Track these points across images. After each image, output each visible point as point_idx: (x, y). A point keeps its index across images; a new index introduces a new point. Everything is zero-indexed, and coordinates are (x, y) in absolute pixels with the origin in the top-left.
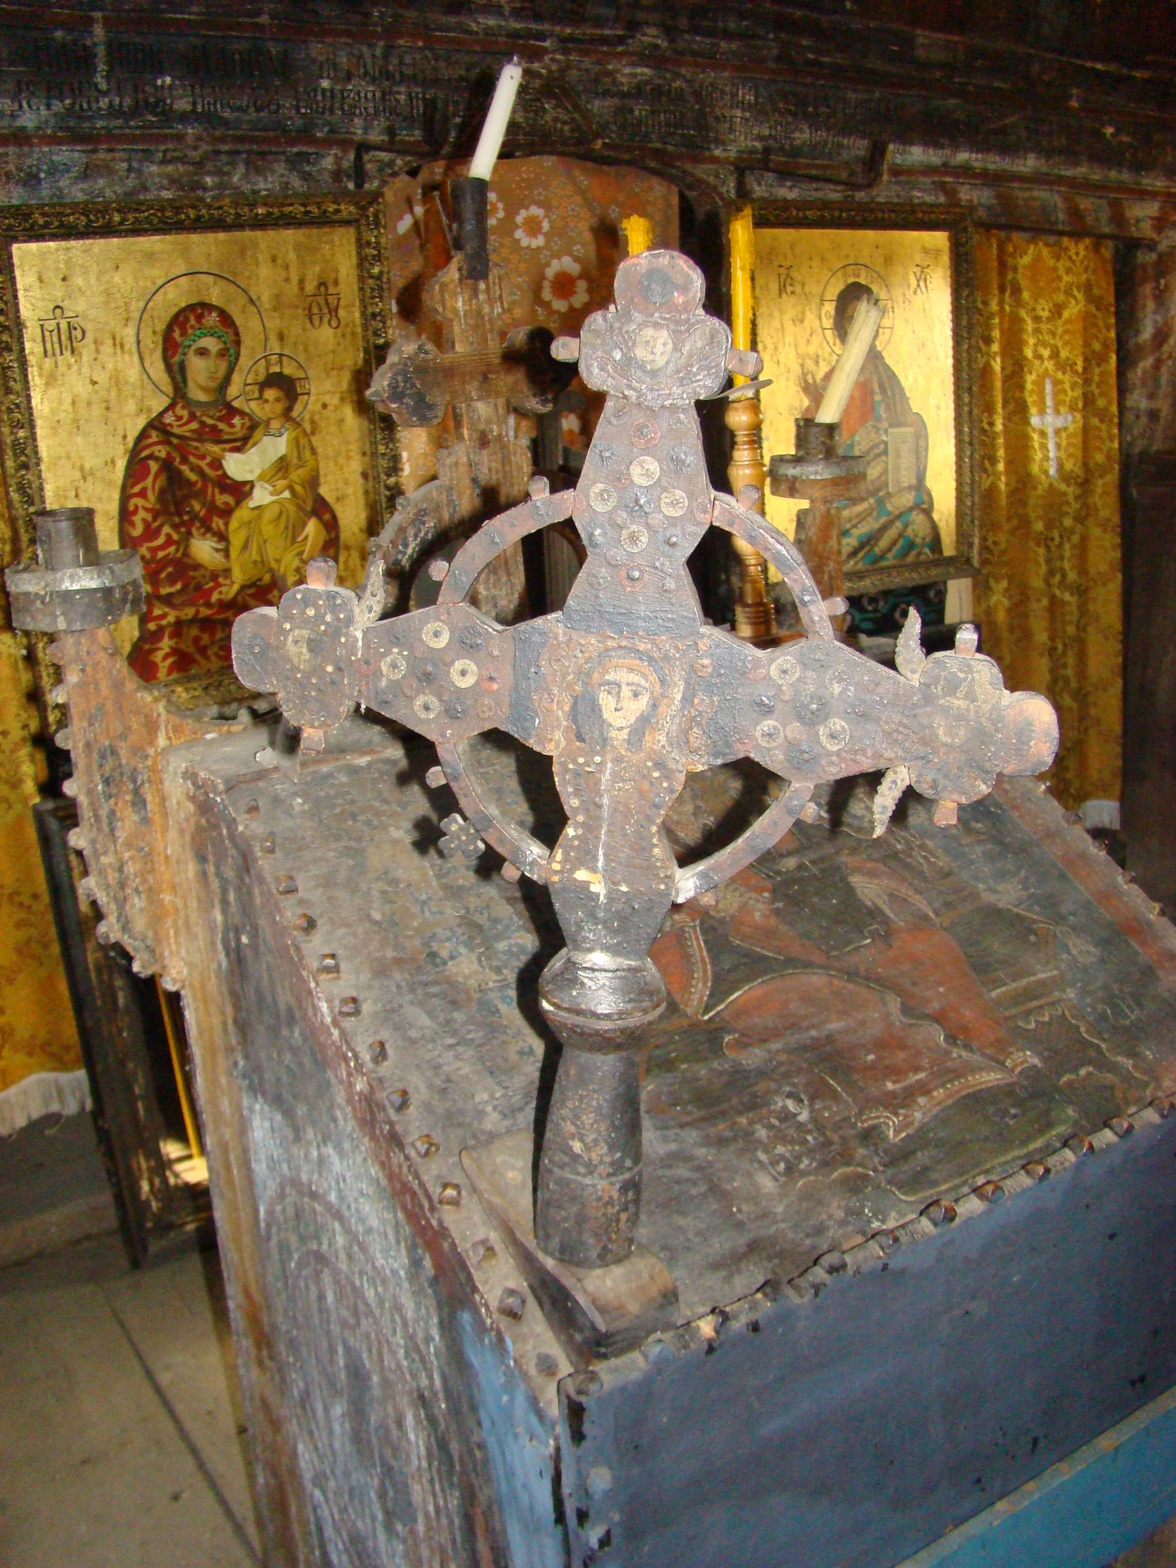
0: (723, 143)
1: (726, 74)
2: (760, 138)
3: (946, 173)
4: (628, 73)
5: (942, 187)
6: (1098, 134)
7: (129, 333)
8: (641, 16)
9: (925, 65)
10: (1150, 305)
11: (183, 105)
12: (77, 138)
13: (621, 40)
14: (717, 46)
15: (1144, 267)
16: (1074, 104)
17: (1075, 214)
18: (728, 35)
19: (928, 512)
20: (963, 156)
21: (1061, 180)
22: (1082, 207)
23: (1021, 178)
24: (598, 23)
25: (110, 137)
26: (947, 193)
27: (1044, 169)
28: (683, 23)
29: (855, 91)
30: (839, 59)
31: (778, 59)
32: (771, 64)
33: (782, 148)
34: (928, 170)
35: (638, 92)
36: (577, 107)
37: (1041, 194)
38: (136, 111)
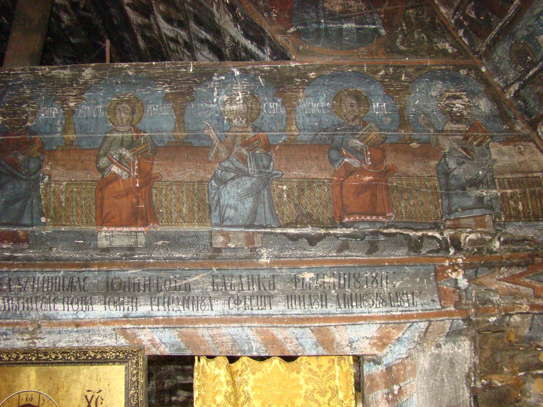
3: (129, 322)
5: (123, 331)
6: (295, 280)
9: (107, 250)
15: (372, 378)
20: (144, 309)
21: (253, 318)
22: (280, 337)
23: (208, 320)
26: (126, 336)
27: (235, 311)
29: (42, 272)
30: (31, 253)
34: (106, 322)
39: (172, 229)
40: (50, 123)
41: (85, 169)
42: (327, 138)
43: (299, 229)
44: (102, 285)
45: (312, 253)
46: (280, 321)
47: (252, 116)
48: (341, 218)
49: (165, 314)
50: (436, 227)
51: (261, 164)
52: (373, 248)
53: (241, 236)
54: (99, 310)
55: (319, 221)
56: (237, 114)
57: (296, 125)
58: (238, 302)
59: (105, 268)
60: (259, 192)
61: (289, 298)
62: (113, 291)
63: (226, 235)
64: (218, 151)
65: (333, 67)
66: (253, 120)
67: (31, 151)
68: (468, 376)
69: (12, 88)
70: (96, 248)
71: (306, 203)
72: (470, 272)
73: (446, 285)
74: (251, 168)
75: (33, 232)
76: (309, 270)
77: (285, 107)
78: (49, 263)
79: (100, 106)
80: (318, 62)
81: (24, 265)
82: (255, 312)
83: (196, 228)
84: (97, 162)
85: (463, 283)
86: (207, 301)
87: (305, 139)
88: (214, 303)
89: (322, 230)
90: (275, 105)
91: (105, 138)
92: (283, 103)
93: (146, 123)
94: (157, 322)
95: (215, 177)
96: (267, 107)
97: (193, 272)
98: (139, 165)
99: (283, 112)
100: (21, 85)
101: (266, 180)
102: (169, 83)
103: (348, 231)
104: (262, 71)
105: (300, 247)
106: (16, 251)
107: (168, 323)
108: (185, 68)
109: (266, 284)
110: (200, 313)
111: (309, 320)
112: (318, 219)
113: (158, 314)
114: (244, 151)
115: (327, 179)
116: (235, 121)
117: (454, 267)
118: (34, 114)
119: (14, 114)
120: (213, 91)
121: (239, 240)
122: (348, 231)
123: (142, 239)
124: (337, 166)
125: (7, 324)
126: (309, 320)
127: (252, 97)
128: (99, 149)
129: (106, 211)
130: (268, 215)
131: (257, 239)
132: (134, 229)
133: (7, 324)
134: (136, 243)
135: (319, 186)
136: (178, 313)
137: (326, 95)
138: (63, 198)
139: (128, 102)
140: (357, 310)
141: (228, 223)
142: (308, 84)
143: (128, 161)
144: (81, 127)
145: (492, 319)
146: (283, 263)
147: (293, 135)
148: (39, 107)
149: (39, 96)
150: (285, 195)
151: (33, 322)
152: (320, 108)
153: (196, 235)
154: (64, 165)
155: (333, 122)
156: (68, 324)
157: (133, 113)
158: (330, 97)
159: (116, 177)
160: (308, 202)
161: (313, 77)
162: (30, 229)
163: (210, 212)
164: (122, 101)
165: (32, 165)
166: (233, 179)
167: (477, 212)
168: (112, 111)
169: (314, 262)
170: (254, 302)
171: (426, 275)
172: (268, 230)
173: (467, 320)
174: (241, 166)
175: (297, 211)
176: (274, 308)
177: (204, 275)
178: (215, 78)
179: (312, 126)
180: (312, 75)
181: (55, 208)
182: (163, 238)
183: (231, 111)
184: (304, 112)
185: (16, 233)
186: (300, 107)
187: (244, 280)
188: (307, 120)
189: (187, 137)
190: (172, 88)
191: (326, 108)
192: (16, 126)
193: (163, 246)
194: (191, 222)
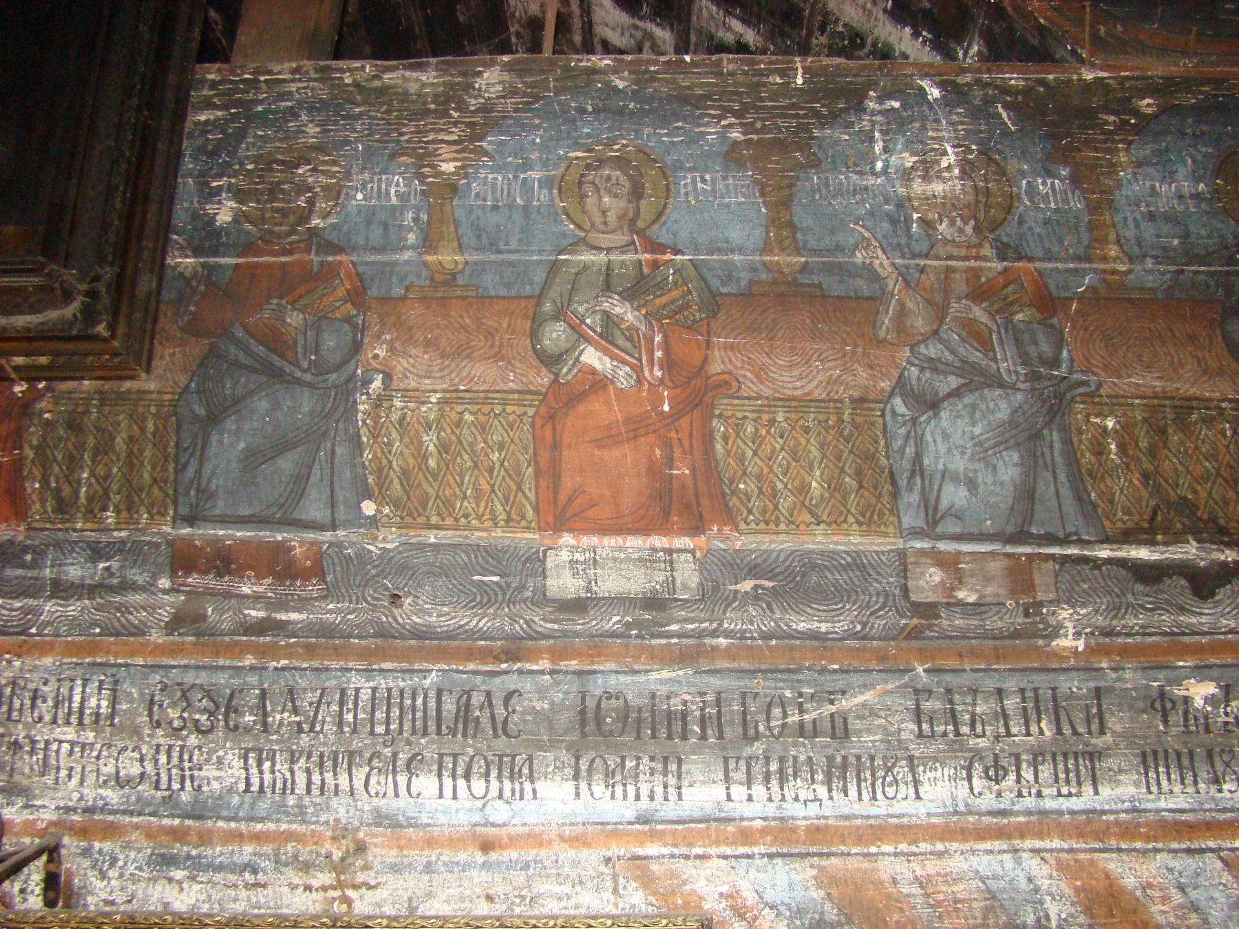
0: (25, 792)
1: (48, 661)
2: (120, 781)
3: (653, 836)
6: (1162, 704)
9: (578, 606)
14: (37, 612)
18: (61, 590)
21: (1043, 823)
22: (1130, 882)
23: (906, 831)
27: (987, 801)
29: (368, 673)
30: (330, 612)
31: (177, 622)
32: (156, 637)
33: (170, 800)
39: (781, 543)
40: (385, 222)
41: (498, 356)
42: (1212, 283)
43: (1163, 548)
44: (566, 718)
45: (1203, 620)
46: (1128, 831)
47: (990, 213)
49: (771, 810)
51: (1032, 350)
53: (995, 566)
54: (555, 799)
55: (1217, 524)
56: (948, 206)
57: (1118, 242)
58: (996, 773)
59: (573, 664)
60: (1035, 436)
61: (1150, 758)
63: (948, 563)
64: (902, 312)
65: (1202, 85)
66: (995, 226)
67: (326, 301)
69: (263, 120)
70: (542, 599)
71: (1176, 470)
74: (1006, 363)
75: (339, 545)
76: (1202, 672)
77: (1083, 193)
78: (388, 644)
79: (535, 175)
80: (1157, 69)
81: (310, 651)
82: (1049, 804)
83: (855, 541)
84: (534, 335)
86: (902, 770)
87: (1149, 285)
88: (925, 775)
89: (1227, 552)
90: (1053, 184)
91: (554, 268)
92: (1075, 181)
93: (679, 224)
94: (746, 836)
95: (901, 385)
96: (1032, 191)
97: (855, 679)
98: (666, 347)
99: (1077, 204)
100: (293, 113)
101: (1055, 403)
102: (738, 114)
104: (1005, 90)
105: (1168, 602)
106: (283, 605)
107: (784, 840)
108: (782, 73)
109: (1079, 717)
110: (881, 808)
111: (1210, 827)
112: (1213, 520)
113: (749, 810)
114: (979, 313)
115: (1231, 401)
116: (942, 227)
118: (334, 192)
119: (271, 192)
120: (871, 139)
121: (988, 579)
123: (688, 575)
125: (258, 838)
126: (1210, 827)
127: (984, 160)
128: (539, 298)
129: (568, 484)
130: (1070, 506)
131: (1043, 576)
132: (659, 541)
133: (258, 838)
134: (671, 584)
135: (1208, 421)
136: (813, 809)
137: (1194, 161)
138: (430, 441)
139: (621, 162)
141: (951, 526)
142: (1138, 130)
143: (631, 335)
144: (479, 231)
146: (1125, 652)
147: (1114, 272)
148: (348, 175)
149: (347, 142)
150: (1113, 447)
151: (341, 832)
152: (1181, 197)
153: (859, 564)
154: (428, 344)
155: (1221, 236)
156: (455, 842)
157: (637, 193)
158: (1205, 168)
159: (597, 383)
160: (1180, 468)
161: (1149, 111)
162: (327, 536)
163: (895, 495)
164: (602, 162)
165: (329, 341)
166: (956, 393)
168: (572, 187)
169: (1214, 649)
170: (1046, 771)
172: (1073, 551)
174: (976, 356)
175: (1151, 494)
176: (1105, 791)
177: (890, 686)
178: (872, 105)
179: (1164, 248)
180: (1147, 104)
181: (405, 472)
182: (754, 571)
183: (928, 199)
184: (1138, 205)
185: (282, 549)
186: (1124, 192)
187: (1011, 703)
188: (1148, 230)
189: (805, 268)
190: (747, 128)
191: (1197, 196)
192: (277, 229)
193: (755, 597)
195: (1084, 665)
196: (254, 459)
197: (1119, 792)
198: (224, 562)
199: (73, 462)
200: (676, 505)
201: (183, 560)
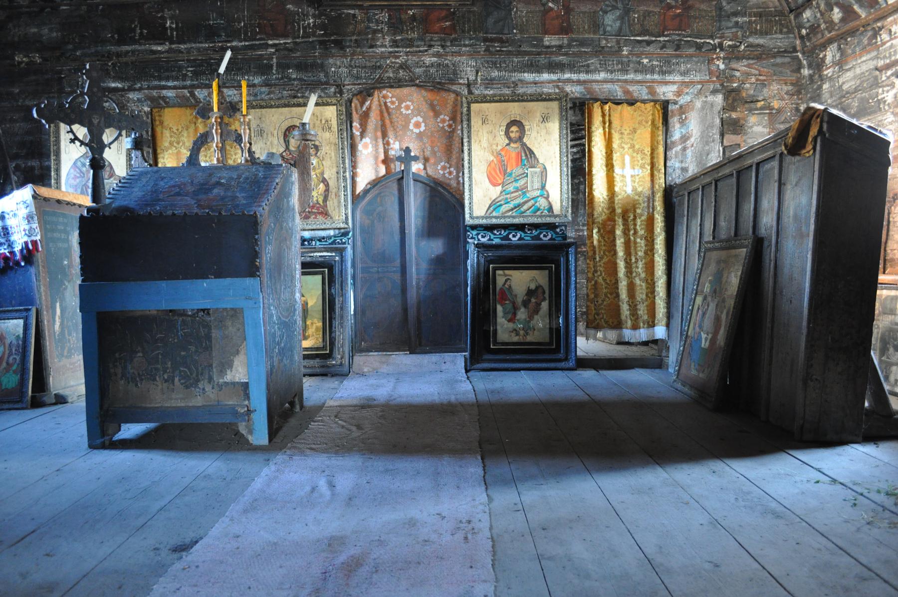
4: (428, 60)
5: (558, 87)
6: (639, 63)
7: (275, 133)
8: (433, 43)
9: (548, 47)
10: (677, 126)
11: (294, 76)
12: (267, 85)
13: (426, 51)
16: (625, 53)
17: (627, 92)
18: (465, 46)
19: (547, 198)
20: (567, 76)
21: (618, 81)
23: (597, 81)
24: (418, 46)
25: (275, 85)
26: (559, 89)
28: (449, 44)
30: (510, 48)
34: (550, 82)
35: (432, 65)
36: (410, 71)
37: (609, 86)
38: (282, 78)
46: (631, 82)
48: (663, 32)
50: (712, 37)
52: (678, 47)
54: (545, 76)
61: (636, 71)
62: (552, 67)
63: (606, 40)
68: (719, 112)
70: (543, 46)
72: (727, 61)
73: (713, 68)
74: (620, 5)
76: (646, 58)
78: (520, 53)
85: (722, 67)
94: (573, 82)
95: (601, 9)
101: (627, 12)
103: (666, 39)
107: (579, 82)
117: (718, 58)
122: (666, 39)
123: (566, 42)
124: (663, 5)
140: (669, 78)
145: (735, 85)
151: (513, 82)
153: (592, 40)
159: (551, 9)
167: (734, 30)
171: (704, 62)
173: (722, 85)
194: (589, 33)
195: (627, 56)
196: (496, 22)
197: (631, 76)
198: (492, 40)
199: (464, 24)
200: (565, 30)
201: (485, 40)
